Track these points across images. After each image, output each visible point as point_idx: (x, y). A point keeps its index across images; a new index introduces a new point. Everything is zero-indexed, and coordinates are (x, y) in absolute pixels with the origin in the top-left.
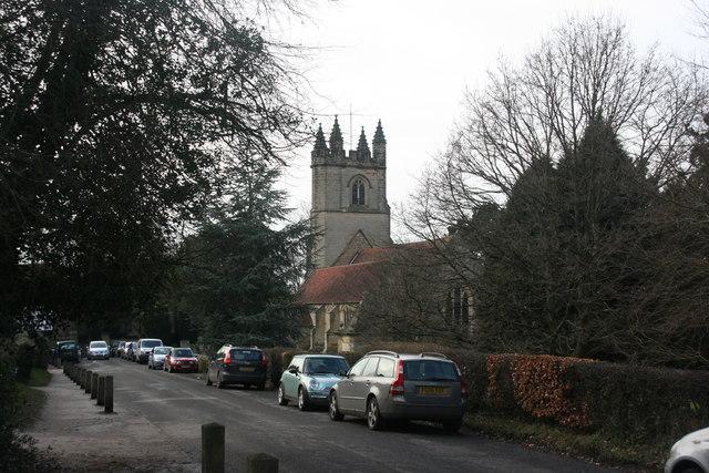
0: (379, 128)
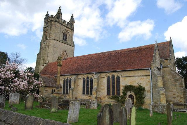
0: (72, 17)
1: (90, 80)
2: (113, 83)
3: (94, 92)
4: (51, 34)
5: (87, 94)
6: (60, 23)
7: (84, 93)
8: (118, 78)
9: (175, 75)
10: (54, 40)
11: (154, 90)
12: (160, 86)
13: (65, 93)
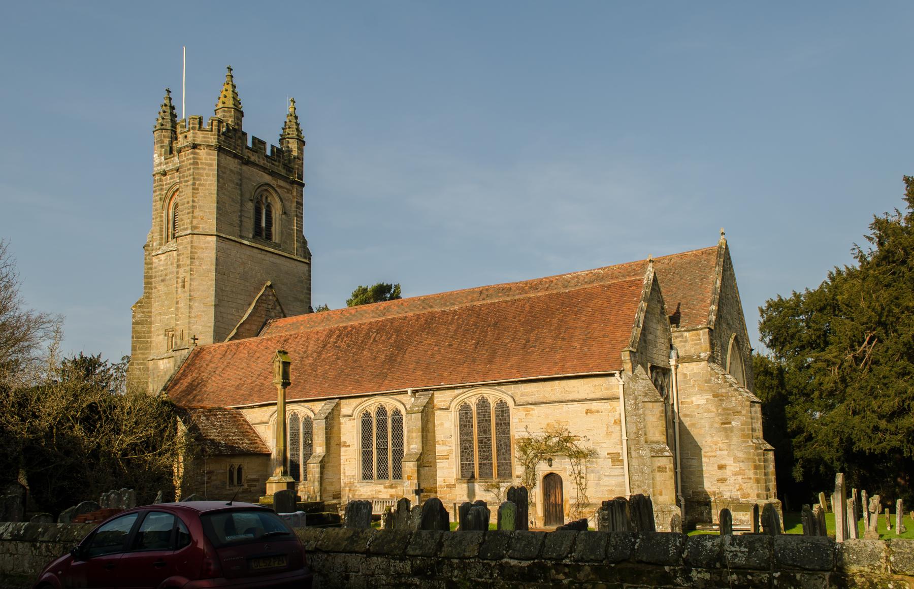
1: (393, 421)
2: (484, 430)
3: (409, 467)
4: (197, 213)
5: (383, 476)
6: (235, 156)
7: (367, 476)
8: (503, 410)
9: (724, 390)
11: (634, 454)
12: (655, 439)
13: (371, 477)
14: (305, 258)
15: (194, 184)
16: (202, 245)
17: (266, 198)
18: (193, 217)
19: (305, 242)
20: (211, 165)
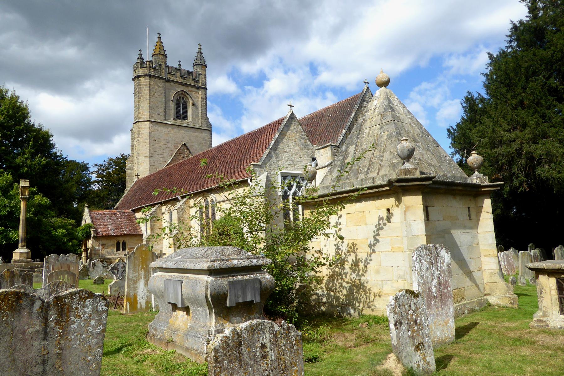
4: (140, 111)
10: (149, 123)
14: (207, 127)
15: (139, 96)
16: (143, 127)
17: (183, 98)
18: (139, 113)
19: (207, 119)
20: (146, 85)
